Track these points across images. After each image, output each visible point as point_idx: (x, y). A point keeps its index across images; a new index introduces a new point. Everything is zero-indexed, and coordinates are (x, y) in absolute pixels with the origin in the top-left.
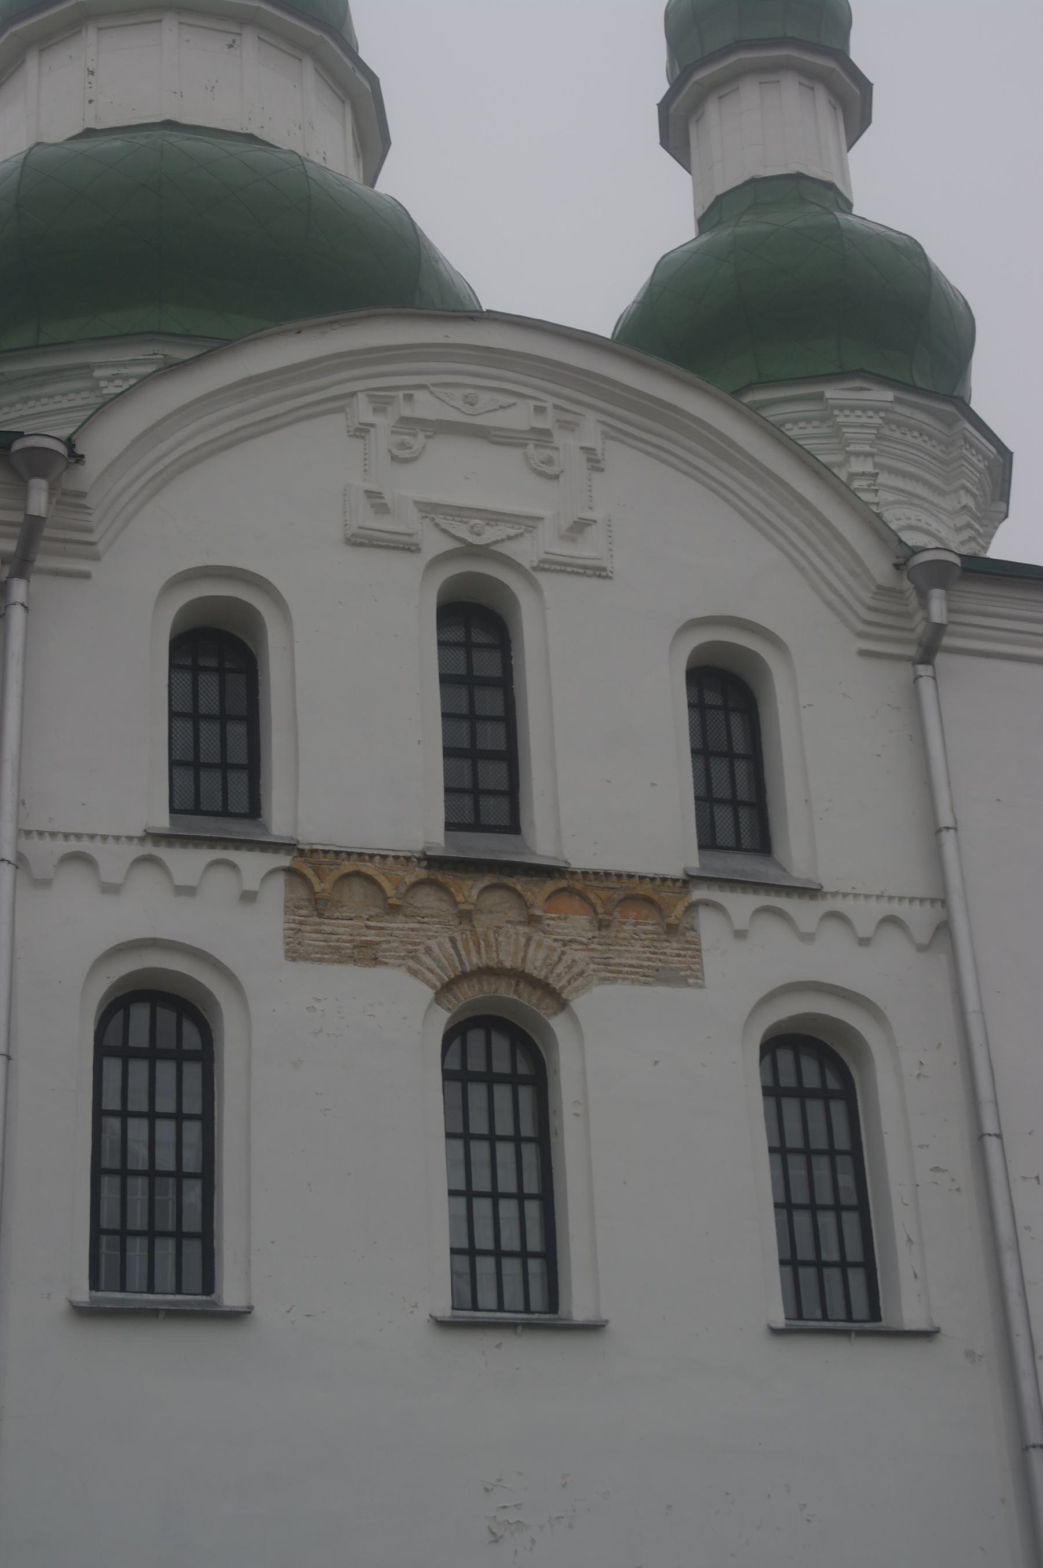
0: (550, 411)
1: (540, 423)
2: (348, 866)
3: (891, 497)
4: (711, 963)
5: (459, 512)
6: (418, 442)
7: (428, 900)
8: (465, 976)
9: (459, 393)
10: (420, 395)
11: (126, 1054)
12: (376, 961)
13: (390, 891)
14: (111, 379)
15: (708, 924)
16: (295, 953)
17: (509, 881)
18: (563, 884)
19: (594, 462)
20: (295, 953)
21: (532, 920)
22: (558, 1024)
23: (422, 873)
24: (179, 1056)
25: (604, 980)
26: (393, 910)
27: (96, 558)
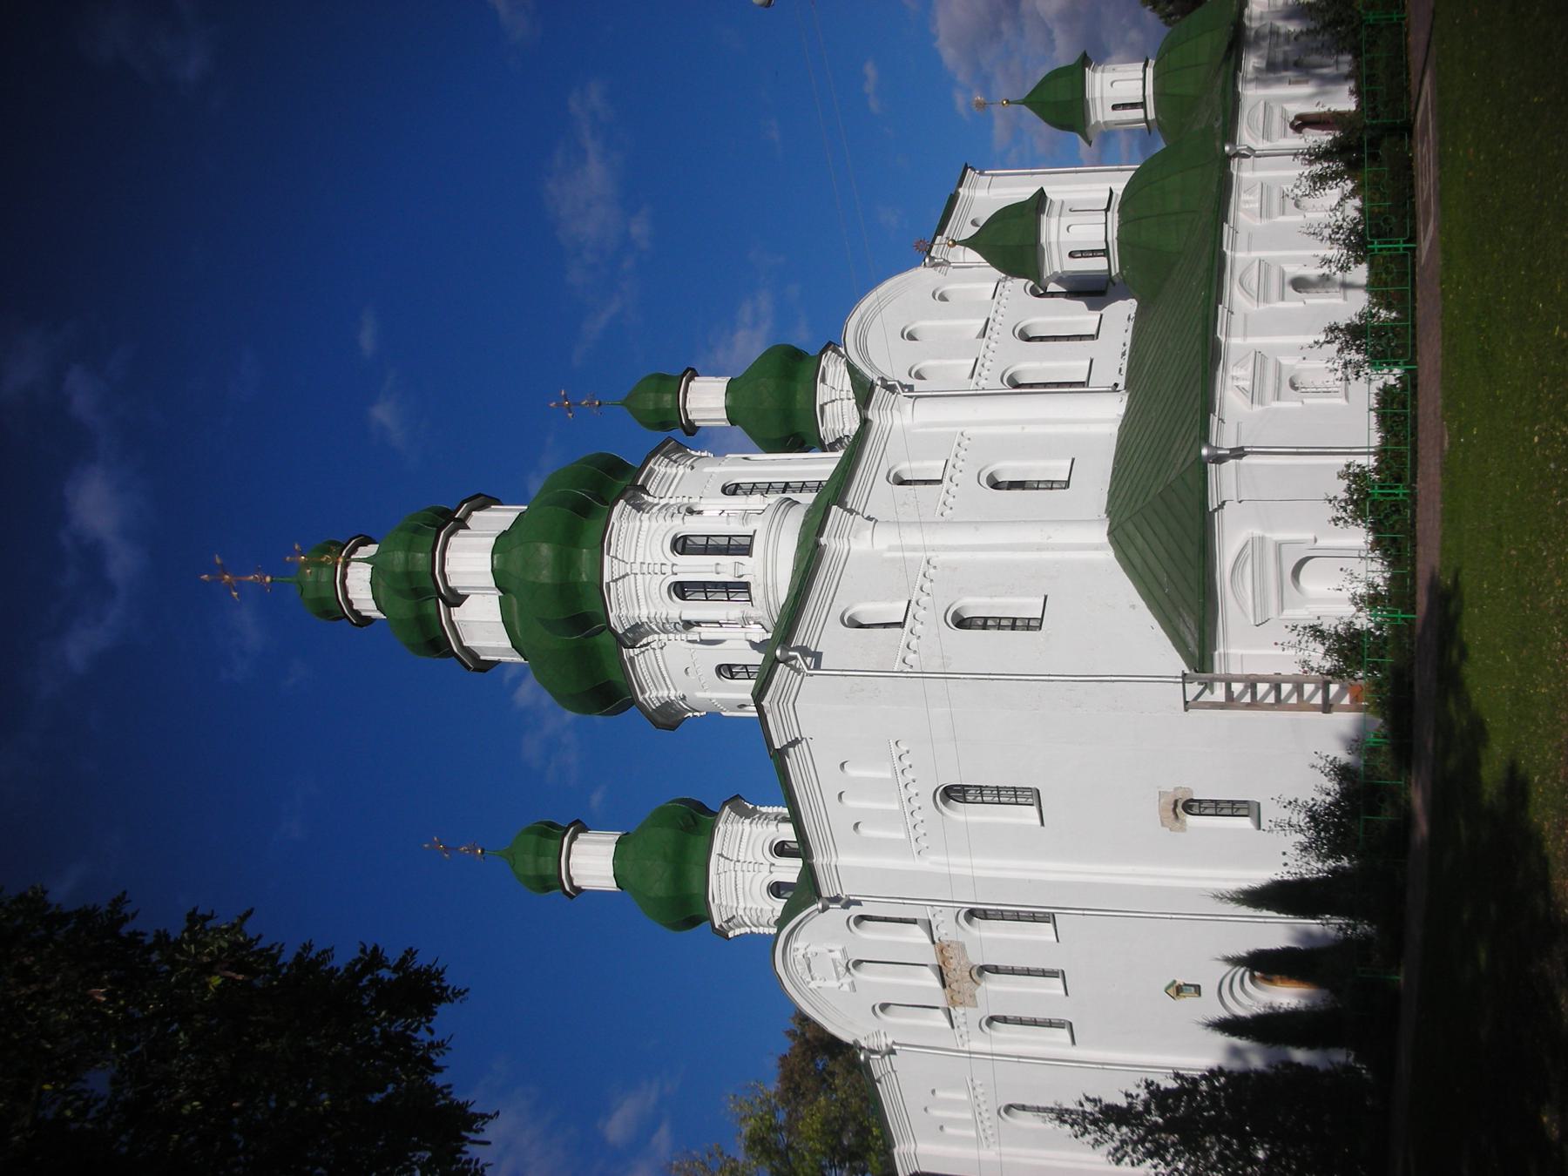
8: (974, 980)
16: (976, 1006)
18: (943, 966)
20: (976, 1006)
27: (879, 1031)
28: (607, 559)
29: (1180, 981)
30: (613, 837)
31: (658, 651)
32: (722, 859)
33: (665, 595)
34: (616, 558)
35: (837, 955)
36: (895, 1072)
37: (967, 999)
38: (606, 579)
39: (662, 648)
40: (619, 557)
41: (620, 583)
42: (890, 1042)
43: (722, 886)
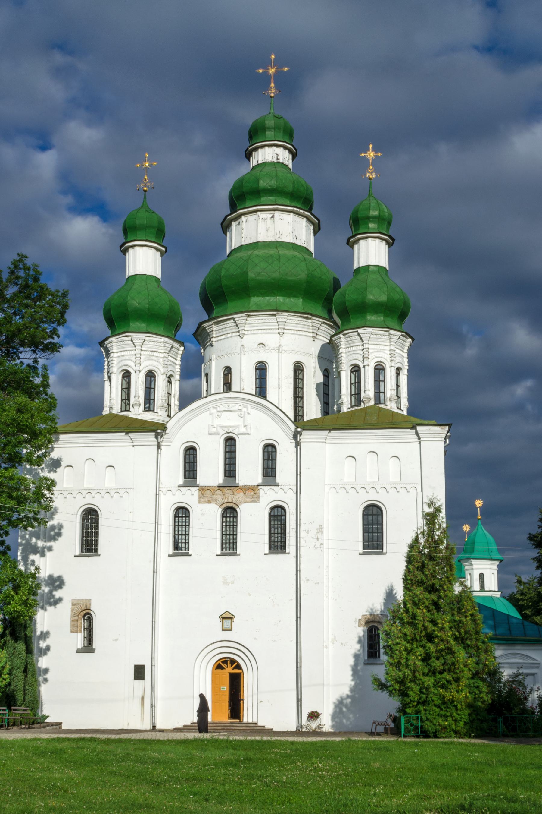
0: (242, 405)
1: (240, 408)
2: (207, 488)
3: (373, 350)
4: (261, 499)
5: (226, 427)
6: (219, 414)
7: (219, 492)
9: (226, 405)
10: (221, 406)
11: (179, 517)
12: (211, 503)
13: (213, 492)
14: (238, 320)
15: (261, 491)
16: (199, 502)
17: (231, 488)
18: (238, 488)
19: (249, 414)
20: (199, 502)
21: (234, 494)
22: (238, 510)
23: (218, 488)
24: (186, 517)
25: (244, 503)
26: (213, 494)
27: (171, 442)
28: (399, 334)
29: (235, 620)
30: (159, 276)
31: (277, 331)
32: (170, 346)
33: (379, 360)
34: (399, 338)
35: (243, 430)
36: (133, 446)
37: (206, 498)
38: (392, 332)
39: (279, 333)
40: (399, 340)
41: (388, 337)
42: (162, 447)
43: (155, 344)
